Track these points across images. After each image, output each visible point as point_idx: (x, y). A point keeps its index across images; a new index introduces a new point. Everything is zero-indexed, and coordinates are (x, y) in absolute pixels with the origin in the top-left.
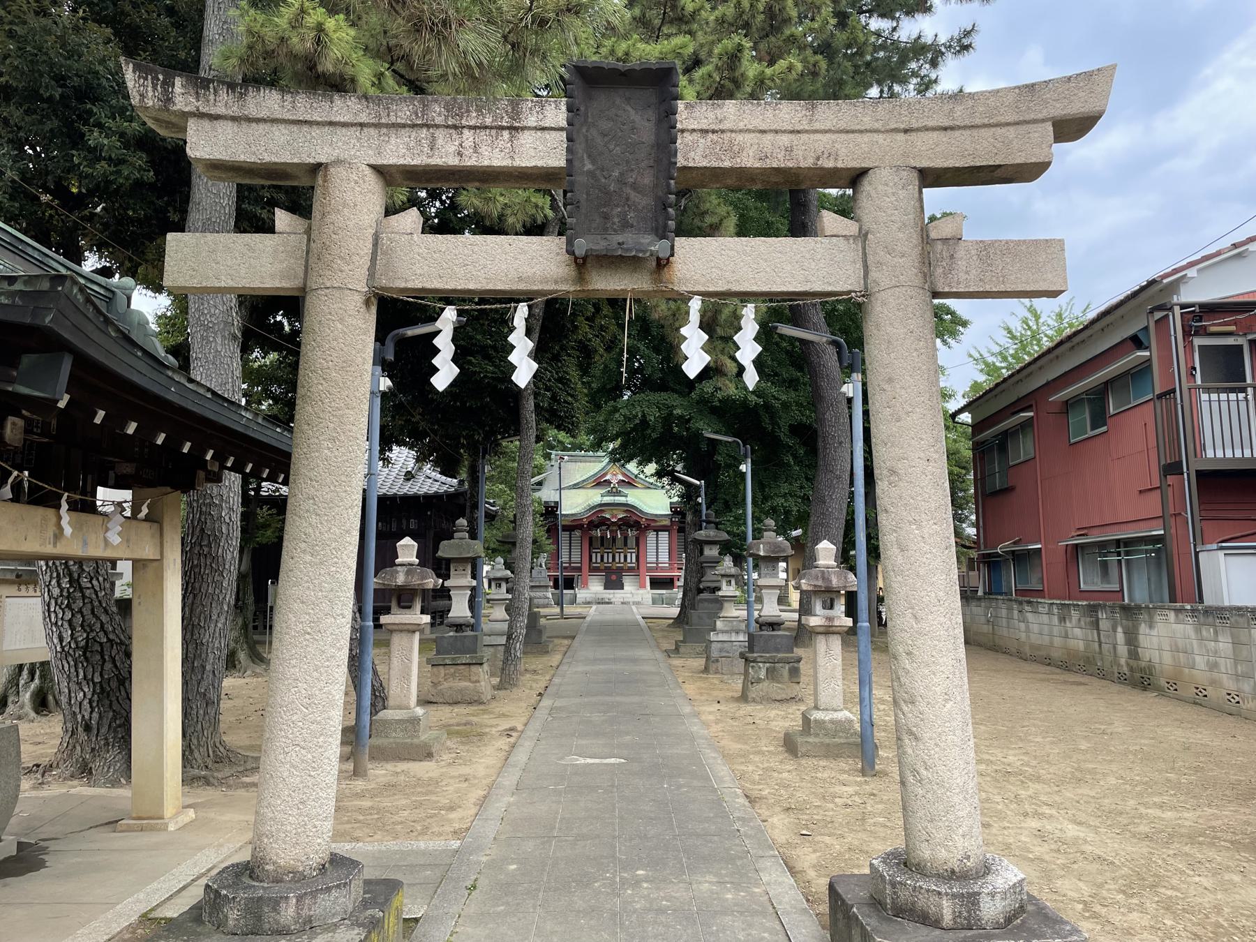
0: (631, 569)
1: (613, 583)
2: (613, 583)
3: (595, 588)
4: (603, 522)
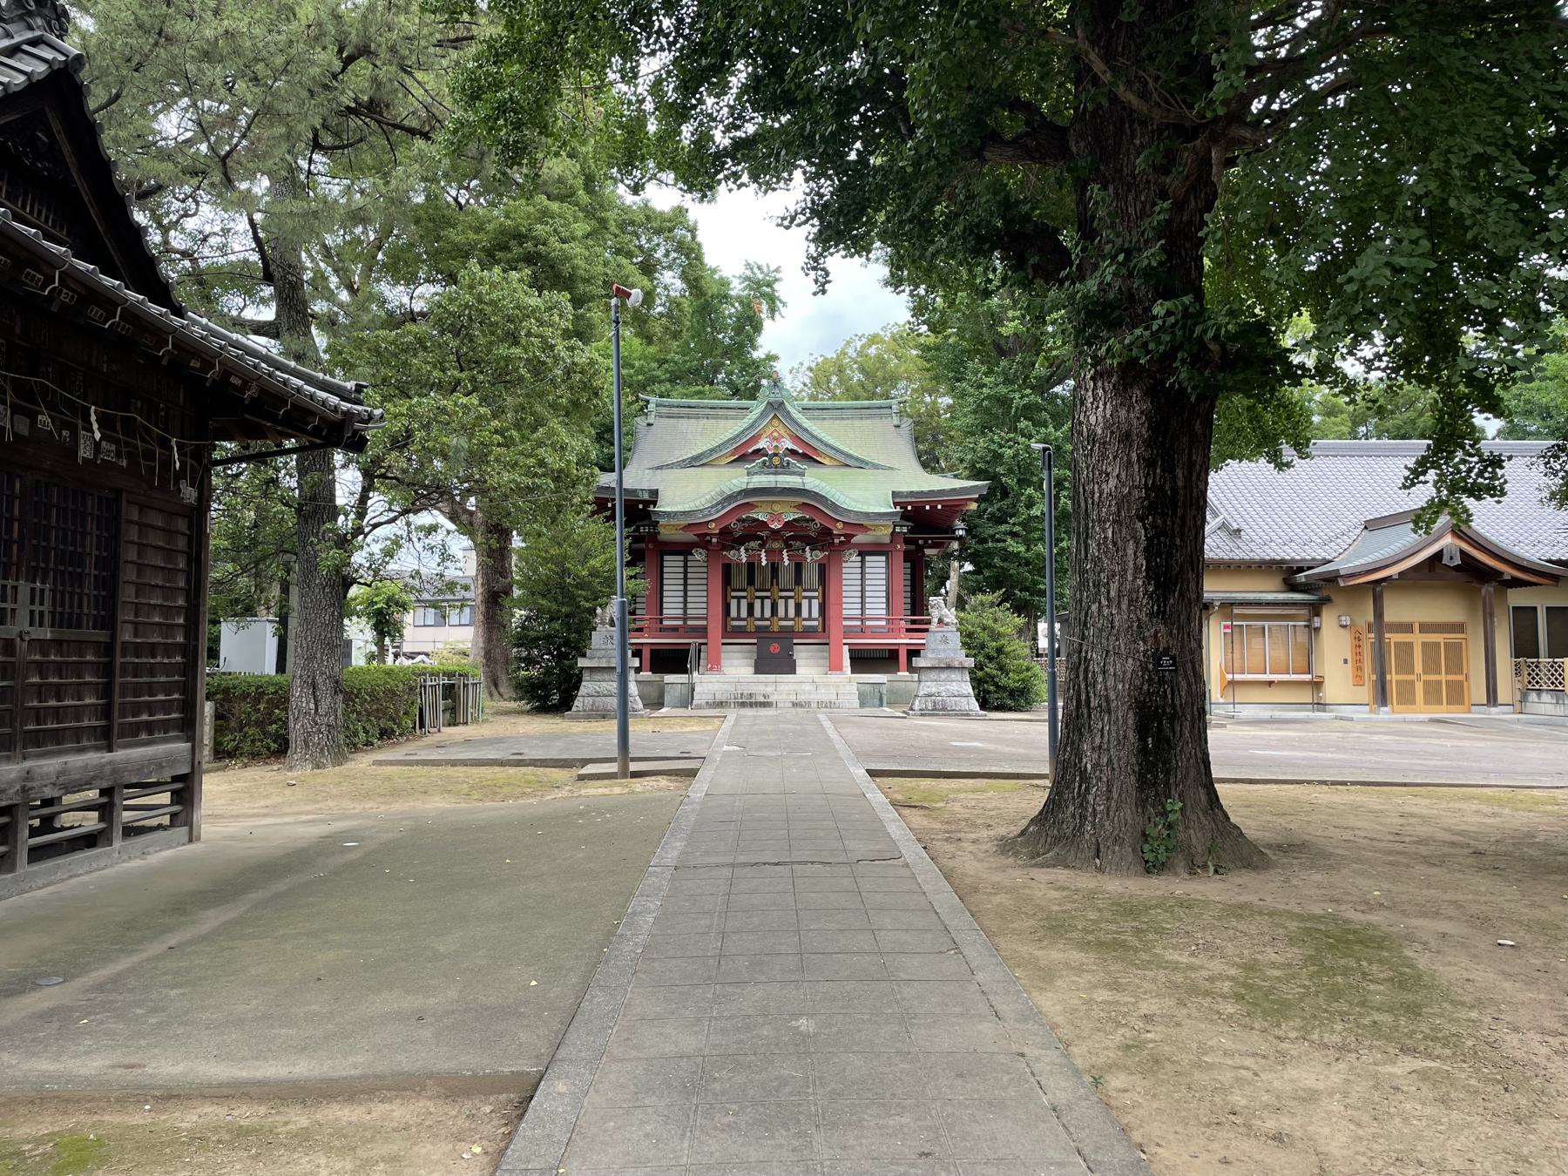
0: (808, 632)
1: (774, 656)
2: (774, 656)
3: (733, 671)
4: (753, 532)
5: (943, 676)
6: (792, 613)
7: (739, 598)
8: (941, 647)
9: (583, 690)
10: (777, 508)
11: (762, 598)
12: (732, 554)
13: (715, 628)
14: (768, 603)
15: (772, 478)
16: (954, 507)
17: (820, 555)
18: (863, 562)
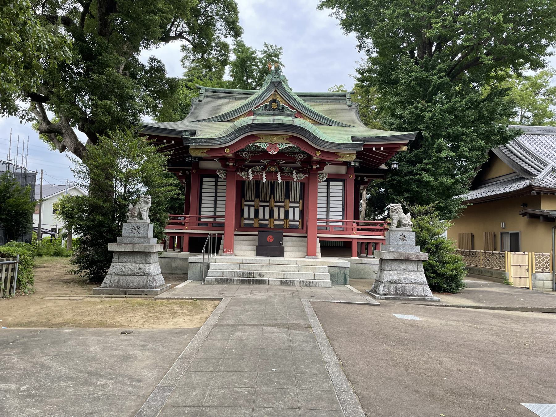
0: (293, 229)
1: (270, 246)
2: (270, 246)
3: (242, 255)
5: (403, 266)
6: (282, 216)
7: (249, 206)
8: (401, 243)
9: (111, 270)
10: (275, 140)
11: (264, 207)
12: (243, 174)
13: (230, 223)
14: (267, 210)
15: (271, 117)
16: (391, 150)
17: (303, 176)
18: (328, 185)
